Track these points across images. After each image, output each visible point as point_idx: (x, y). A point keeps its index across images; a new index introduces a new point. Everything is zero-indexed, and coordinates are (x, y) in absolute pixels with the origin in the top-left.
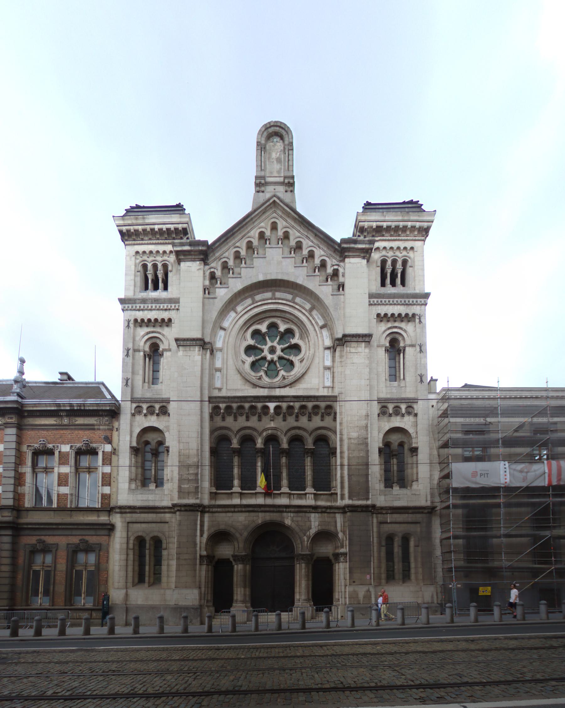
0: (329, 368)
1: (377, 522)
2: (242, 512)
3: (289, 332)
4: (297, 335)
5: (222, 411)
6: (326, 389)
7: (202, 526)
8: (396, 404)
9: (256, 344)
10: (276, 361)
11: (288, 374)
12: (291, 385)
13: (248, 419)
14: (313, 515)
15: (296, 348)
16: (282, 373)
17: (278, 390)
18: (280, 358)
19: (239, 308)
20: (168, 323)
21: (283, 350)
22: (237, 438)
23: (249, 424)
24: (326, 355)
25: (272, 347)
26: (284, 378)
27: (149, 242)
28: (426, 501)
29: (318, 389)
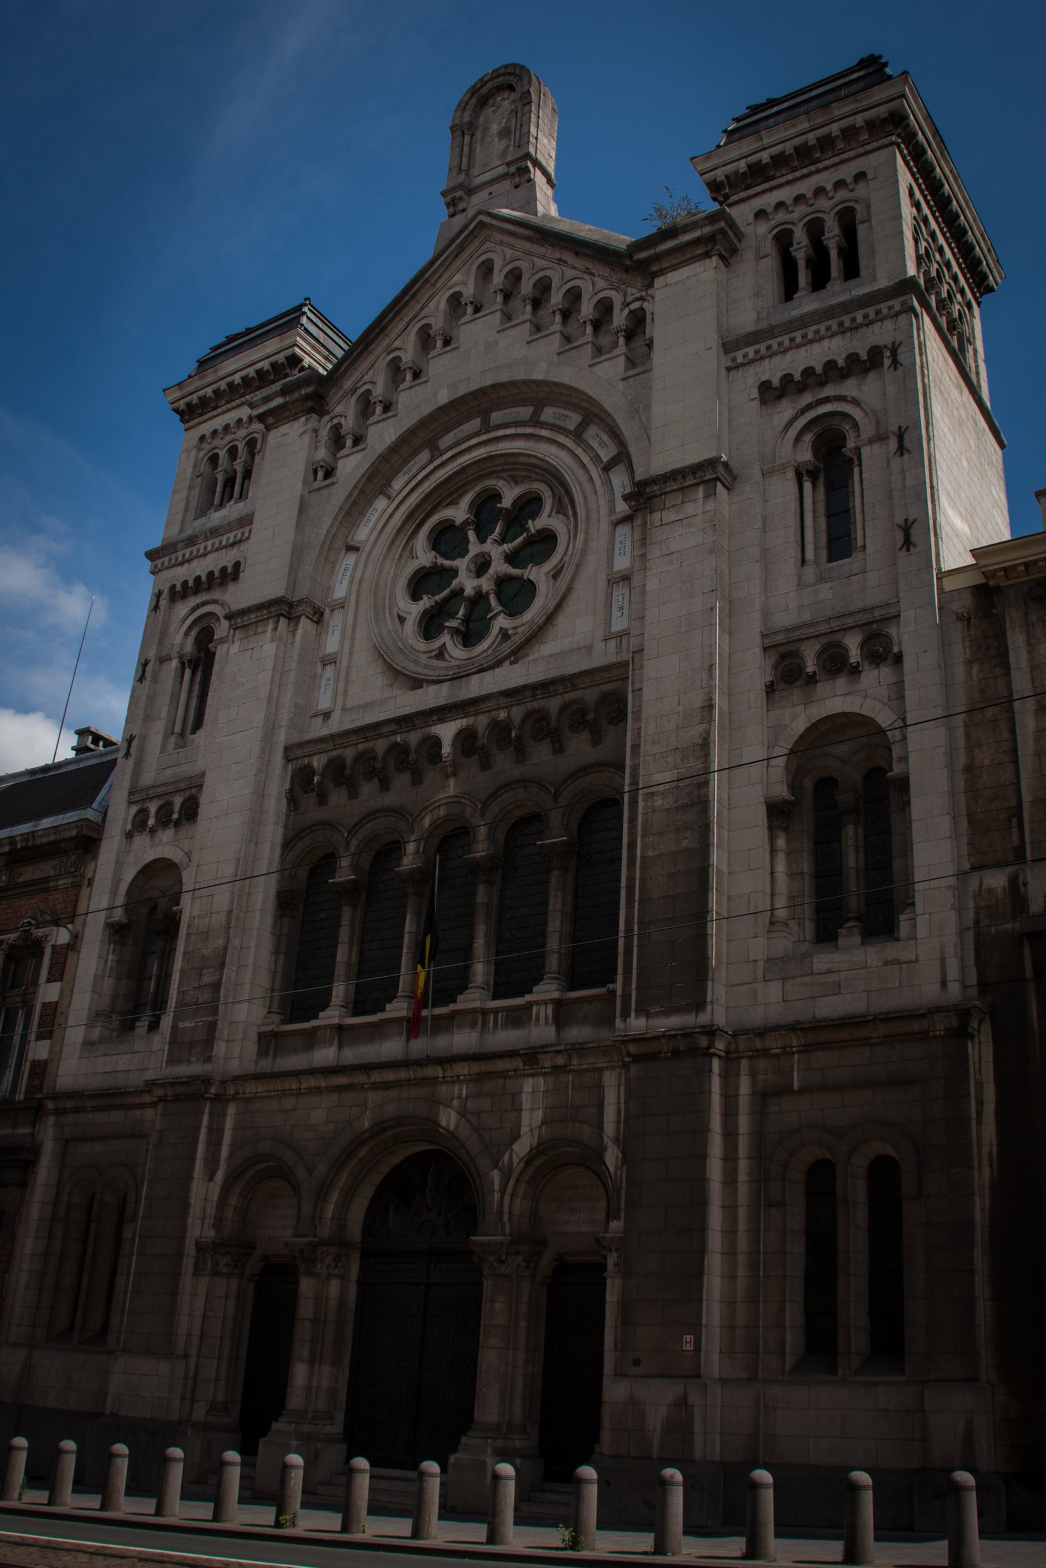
0: (626, 578)
1: (753, 1094)
2: (318, 1090)
3: (529, 505)
4: (548, 504)
5: (316, 779)
6: (612, 644)
7: (215, 1144)
8: (825, 640)
9: (441, 561)
10: (488, 593)
11: (518, 621)
12: (516, 655)
13: (385, 785)
14: (528, 1085)
15: (547, 539)
16: (502, 622)
17: (475, 679)
18: (501, 581)
19: (397, 484)
20: (231, 575)
21: (511, 559)
22: (352, 849)
23: (389, 799)
24: (618, 540)
25: (482, 554)
26: (505, 635)
27: (229, 406)
28: (944, 984)
29: (589, 648)
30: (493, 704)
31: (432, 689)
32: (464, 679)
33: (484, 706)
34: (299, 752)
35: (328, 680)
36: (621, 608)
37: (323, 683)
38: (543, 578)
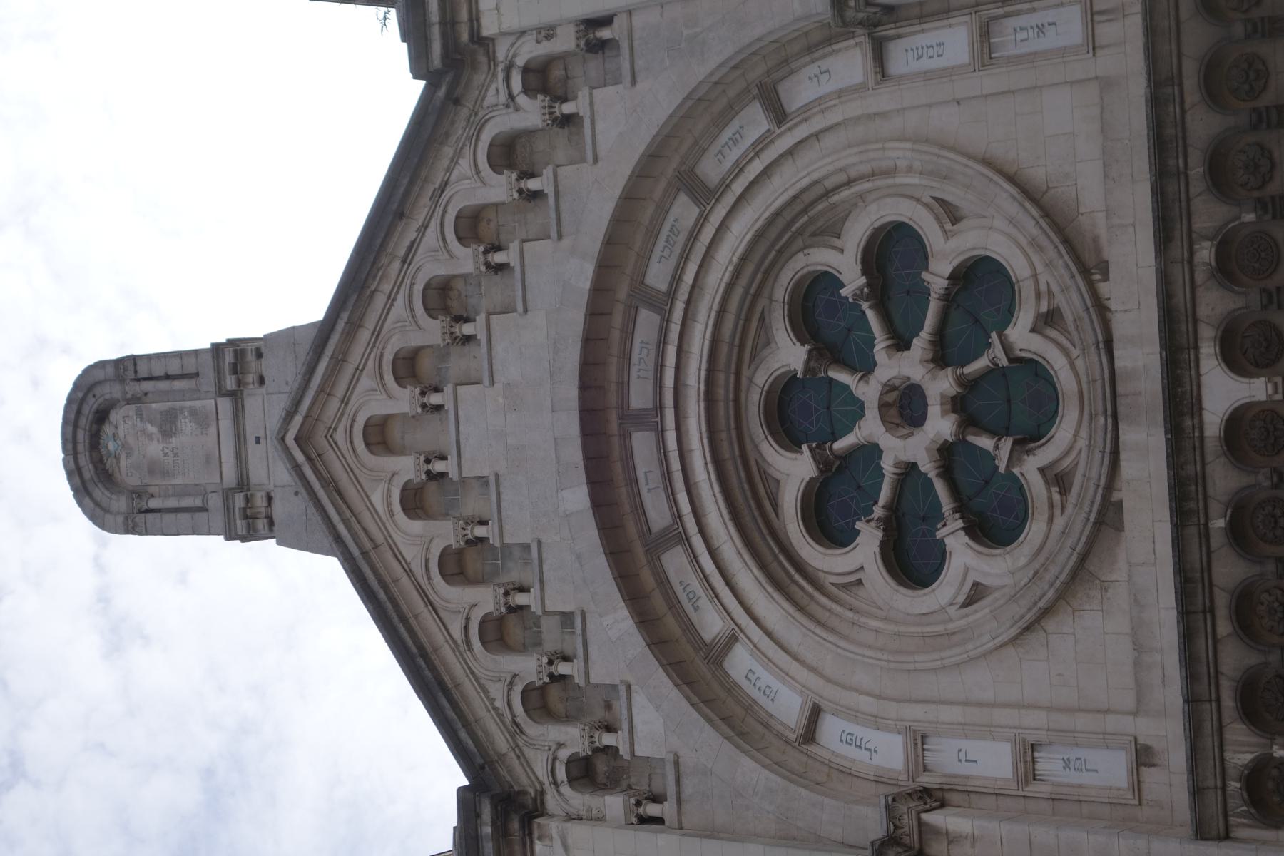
30: (1179, 274)
31: (1128, 468)
32: (1120, 389)
33: (1180, 299)
34: (1213, 801)
35: (1067, 763)
36: (1041, 29)
37: (1073, 777)
38: (953, 243)
